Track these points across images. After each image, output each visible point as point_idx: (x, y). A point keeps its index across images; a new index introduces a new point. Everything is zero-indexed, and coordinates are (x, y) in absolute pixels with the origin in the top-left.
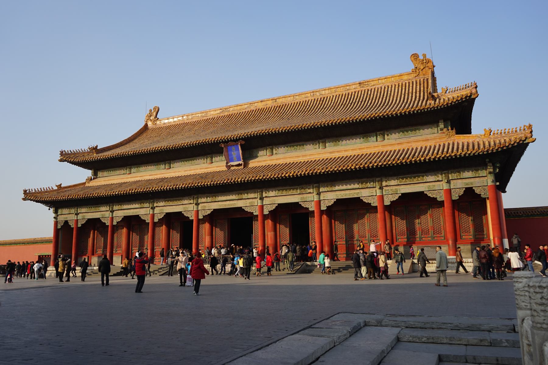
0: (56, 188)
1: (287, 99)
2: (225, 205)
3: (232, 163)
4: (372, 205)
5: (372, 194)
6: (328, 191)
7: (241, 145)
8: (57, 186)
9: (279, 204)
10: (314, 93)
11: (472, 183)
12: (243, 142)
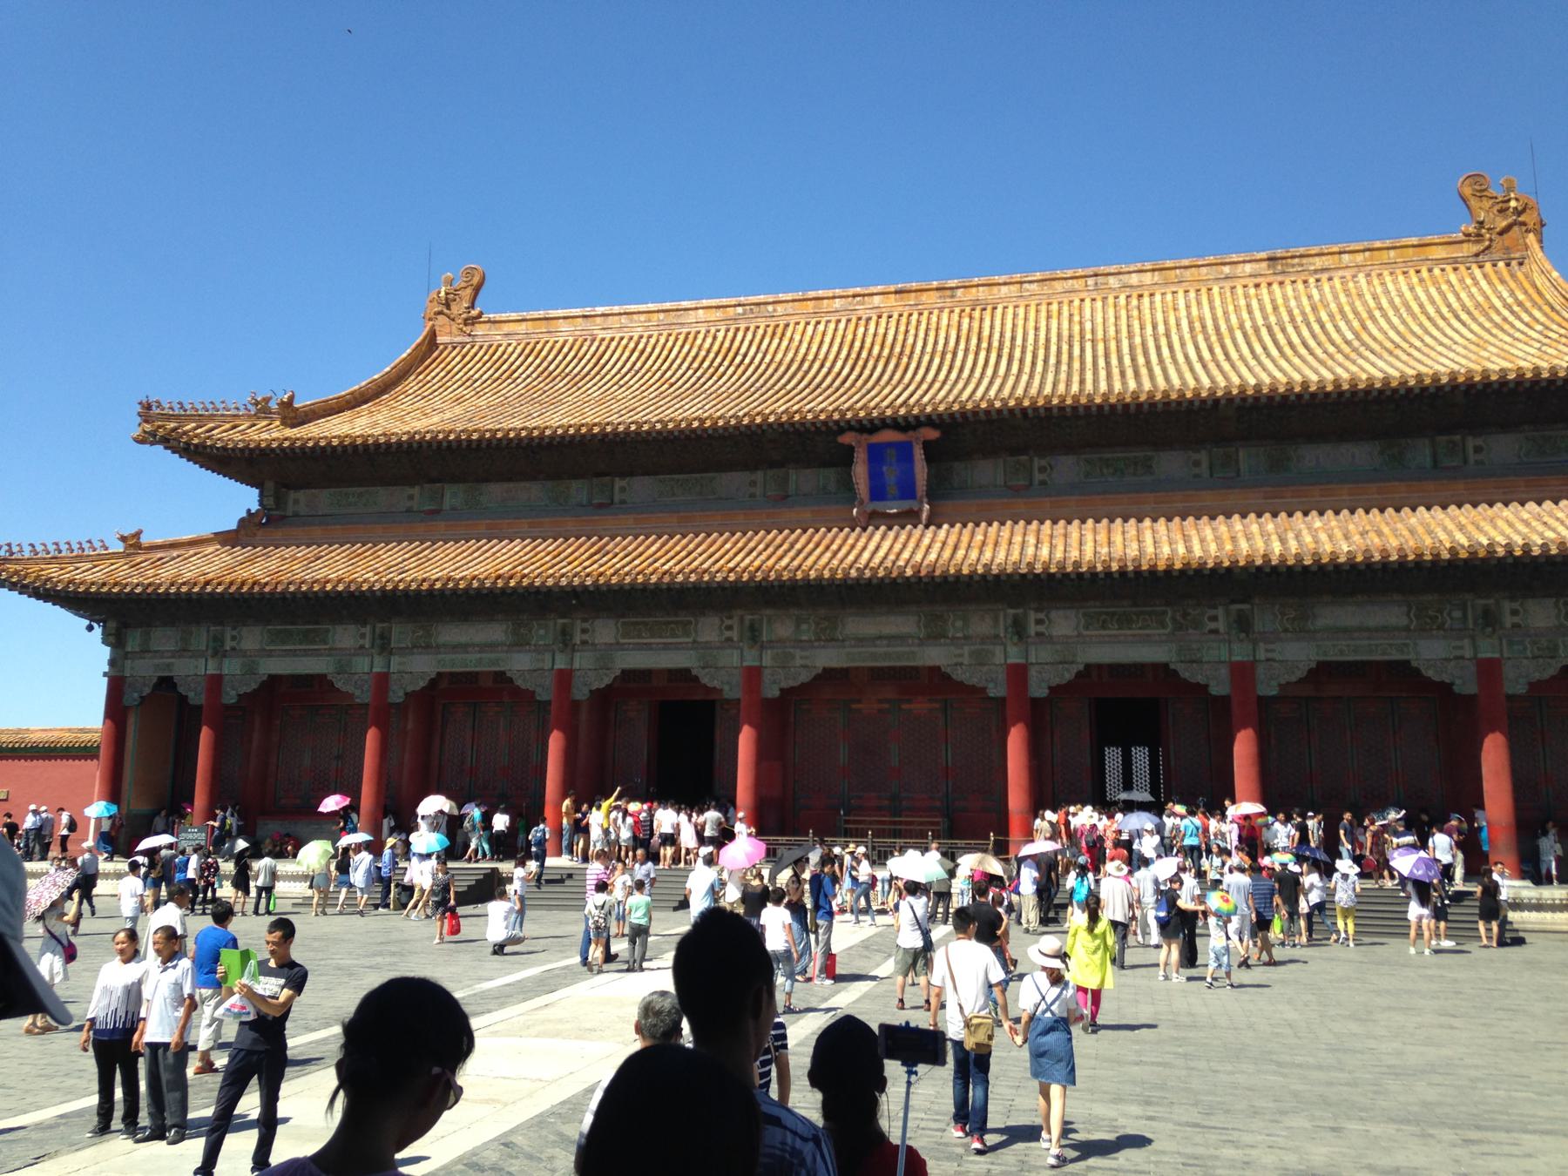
0: (119, 547)
1: (995, 289)
4: (1456, 689)
5: (1458, 653)
6: (1286, 630)
7: (927, 446)
8: (123, 539)
10: (1100, 280)
12: (933, 434)
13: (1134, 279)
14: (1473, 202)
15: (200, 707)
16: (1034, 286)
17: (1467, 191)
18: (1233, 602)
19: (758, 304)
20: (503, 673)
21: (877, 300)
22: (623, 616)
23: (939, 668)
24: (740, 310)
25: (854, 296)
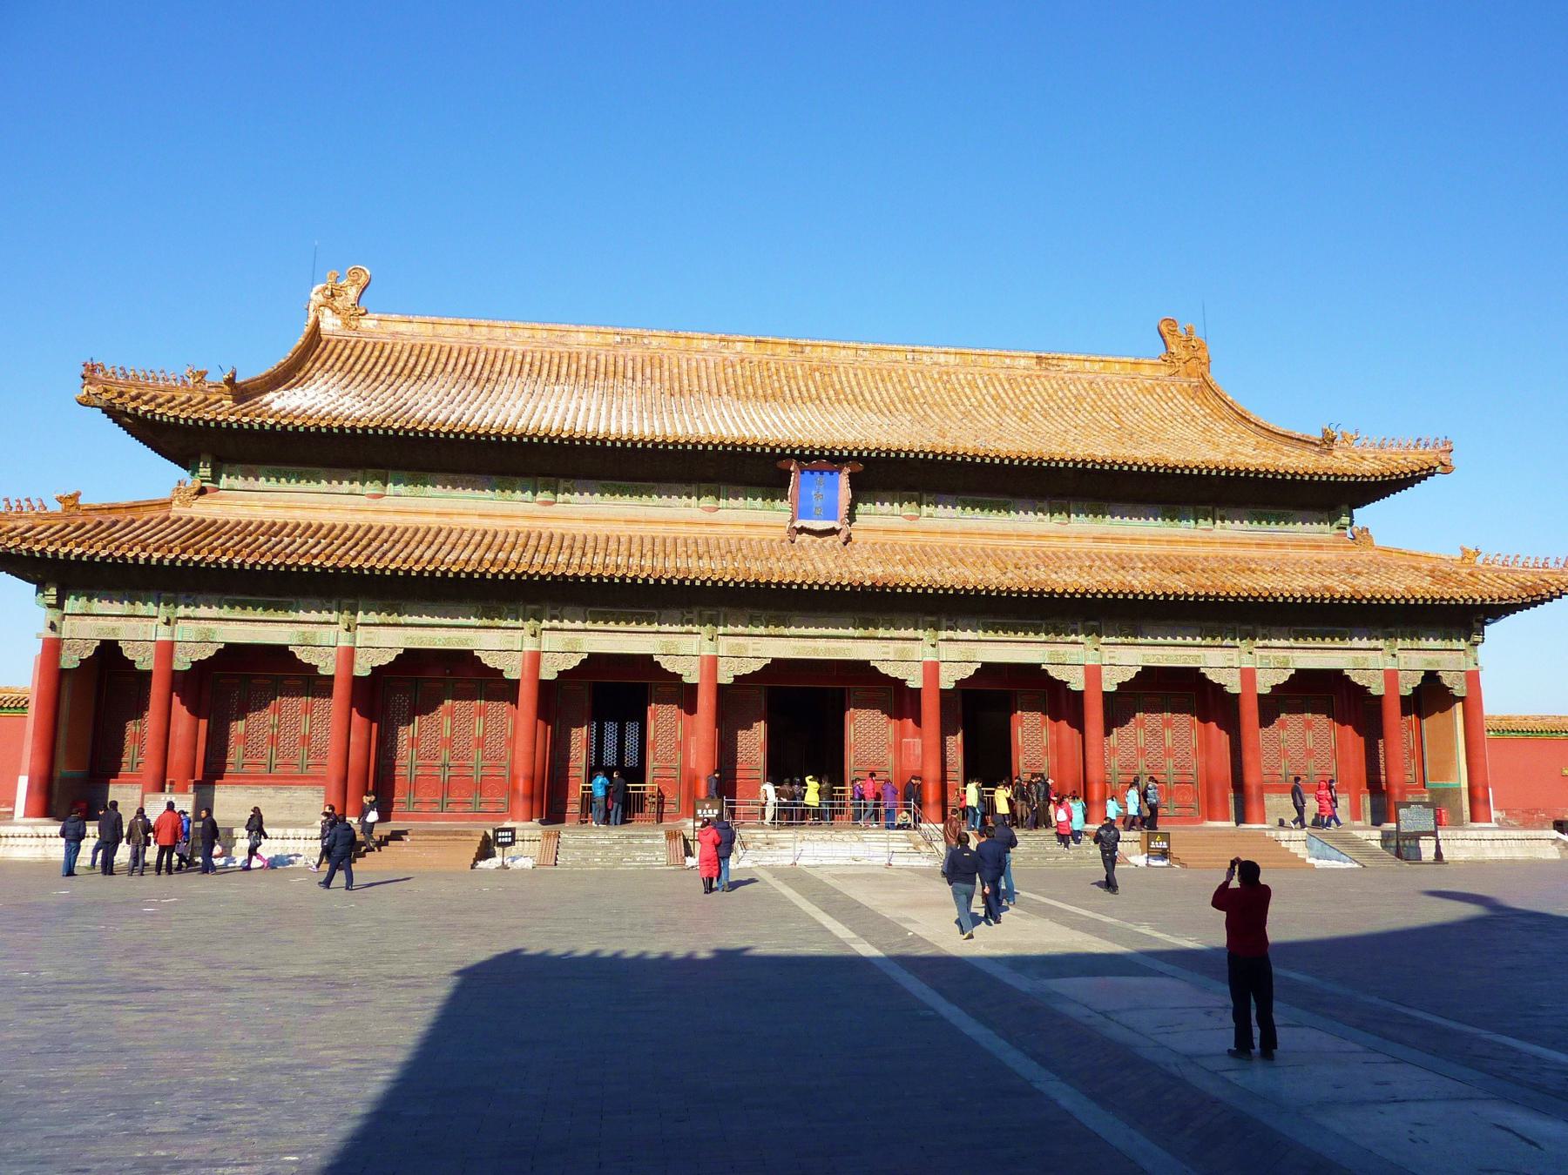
0: (58, 508)
1: (836, 351)
2: (815, 650)
3: (808, 524)
4: (1228, 689)
7: (851, 476)
8: (60, 500)
9: (984, 664)
10: (917, 356)
11: (1438, 663)
13: (942, 359)
14: (1168, 338)
15: (149, 673)
16: (866, 354)
17: (1164, 329)
18: (1088, 619)
19: (635, 336)
20: (471, 652)
21: (739, 346)
22: (590, 605)
23: (868, 662)
24: (618, 338)
25: (721, 340)
